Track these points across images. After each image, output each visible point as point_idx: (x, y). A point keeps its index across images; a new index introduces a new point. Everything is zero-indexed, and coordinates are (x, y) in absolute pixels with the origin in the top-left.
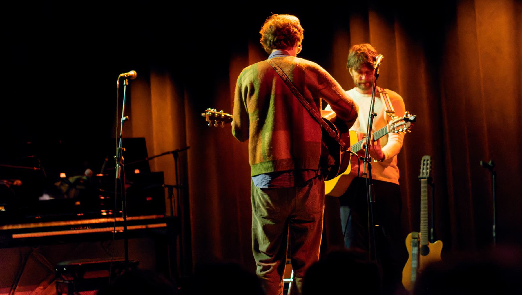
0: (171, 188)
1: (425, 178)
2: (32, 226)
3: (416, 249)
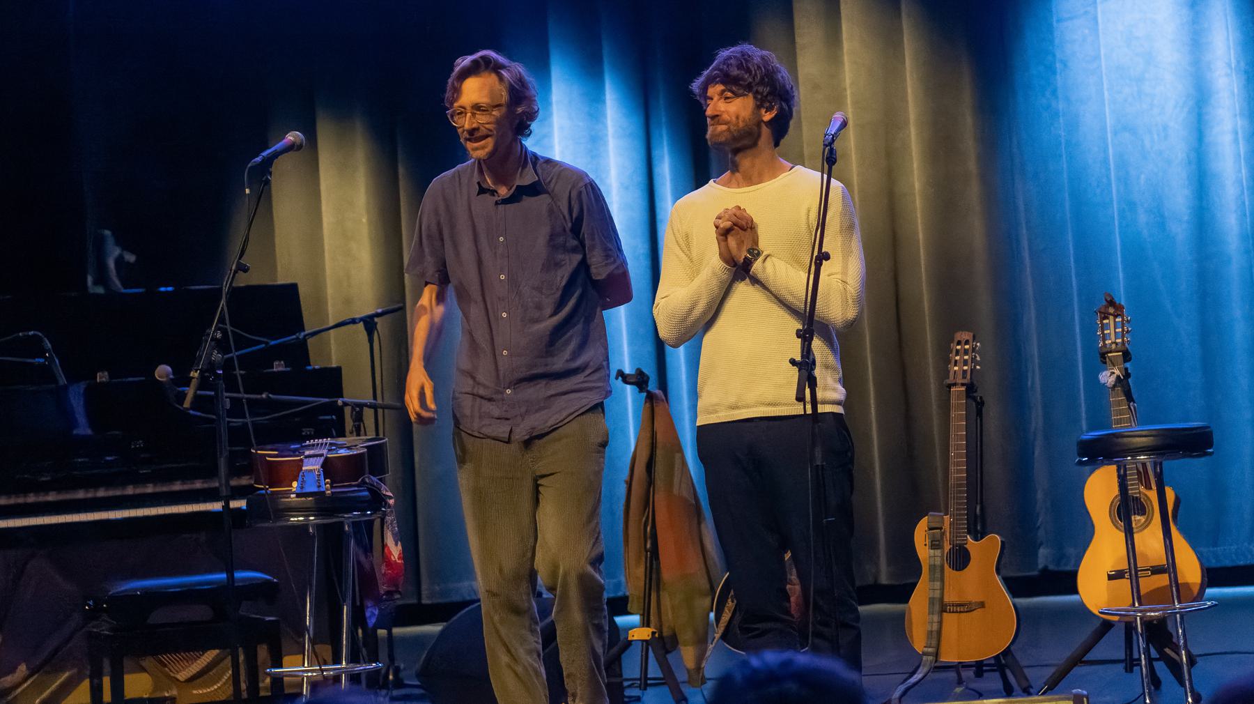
0: (358, 409)
1: (963, 385)
2: (31, 499)
3: (938, 552)
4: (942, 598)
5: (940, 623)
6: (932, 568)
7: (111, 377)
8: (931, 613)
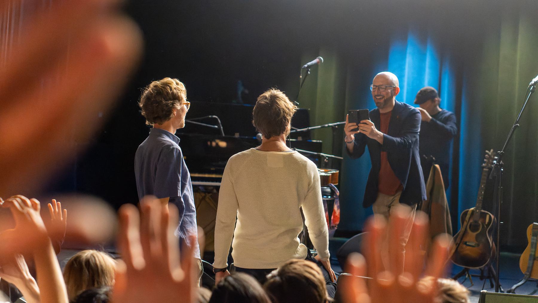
2: (207, 176)
4: (534, 255)
5: (533, 263)
6: (532, 243)
7: (240, 135)
8: (530, 260)
